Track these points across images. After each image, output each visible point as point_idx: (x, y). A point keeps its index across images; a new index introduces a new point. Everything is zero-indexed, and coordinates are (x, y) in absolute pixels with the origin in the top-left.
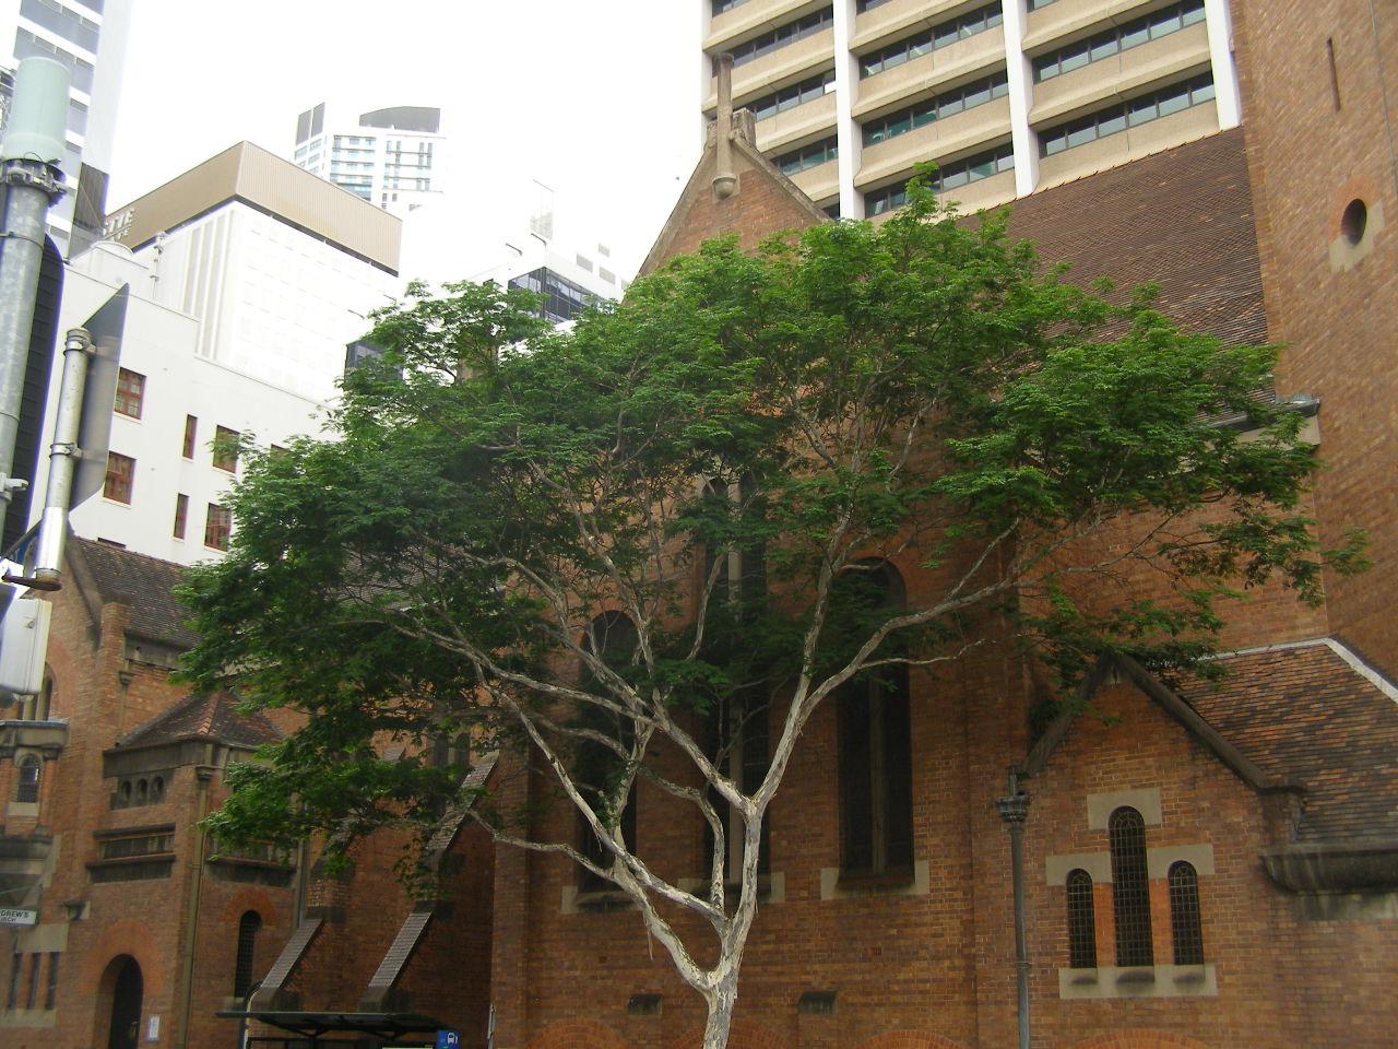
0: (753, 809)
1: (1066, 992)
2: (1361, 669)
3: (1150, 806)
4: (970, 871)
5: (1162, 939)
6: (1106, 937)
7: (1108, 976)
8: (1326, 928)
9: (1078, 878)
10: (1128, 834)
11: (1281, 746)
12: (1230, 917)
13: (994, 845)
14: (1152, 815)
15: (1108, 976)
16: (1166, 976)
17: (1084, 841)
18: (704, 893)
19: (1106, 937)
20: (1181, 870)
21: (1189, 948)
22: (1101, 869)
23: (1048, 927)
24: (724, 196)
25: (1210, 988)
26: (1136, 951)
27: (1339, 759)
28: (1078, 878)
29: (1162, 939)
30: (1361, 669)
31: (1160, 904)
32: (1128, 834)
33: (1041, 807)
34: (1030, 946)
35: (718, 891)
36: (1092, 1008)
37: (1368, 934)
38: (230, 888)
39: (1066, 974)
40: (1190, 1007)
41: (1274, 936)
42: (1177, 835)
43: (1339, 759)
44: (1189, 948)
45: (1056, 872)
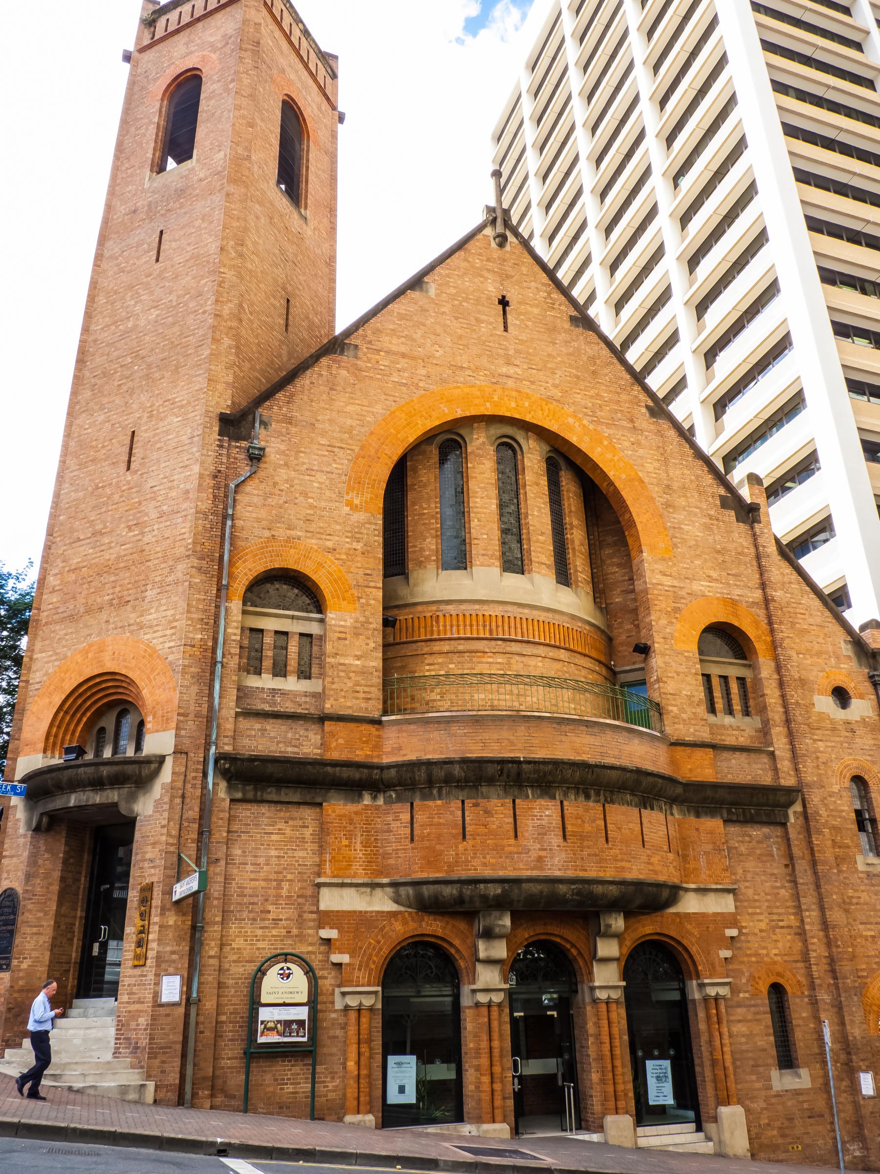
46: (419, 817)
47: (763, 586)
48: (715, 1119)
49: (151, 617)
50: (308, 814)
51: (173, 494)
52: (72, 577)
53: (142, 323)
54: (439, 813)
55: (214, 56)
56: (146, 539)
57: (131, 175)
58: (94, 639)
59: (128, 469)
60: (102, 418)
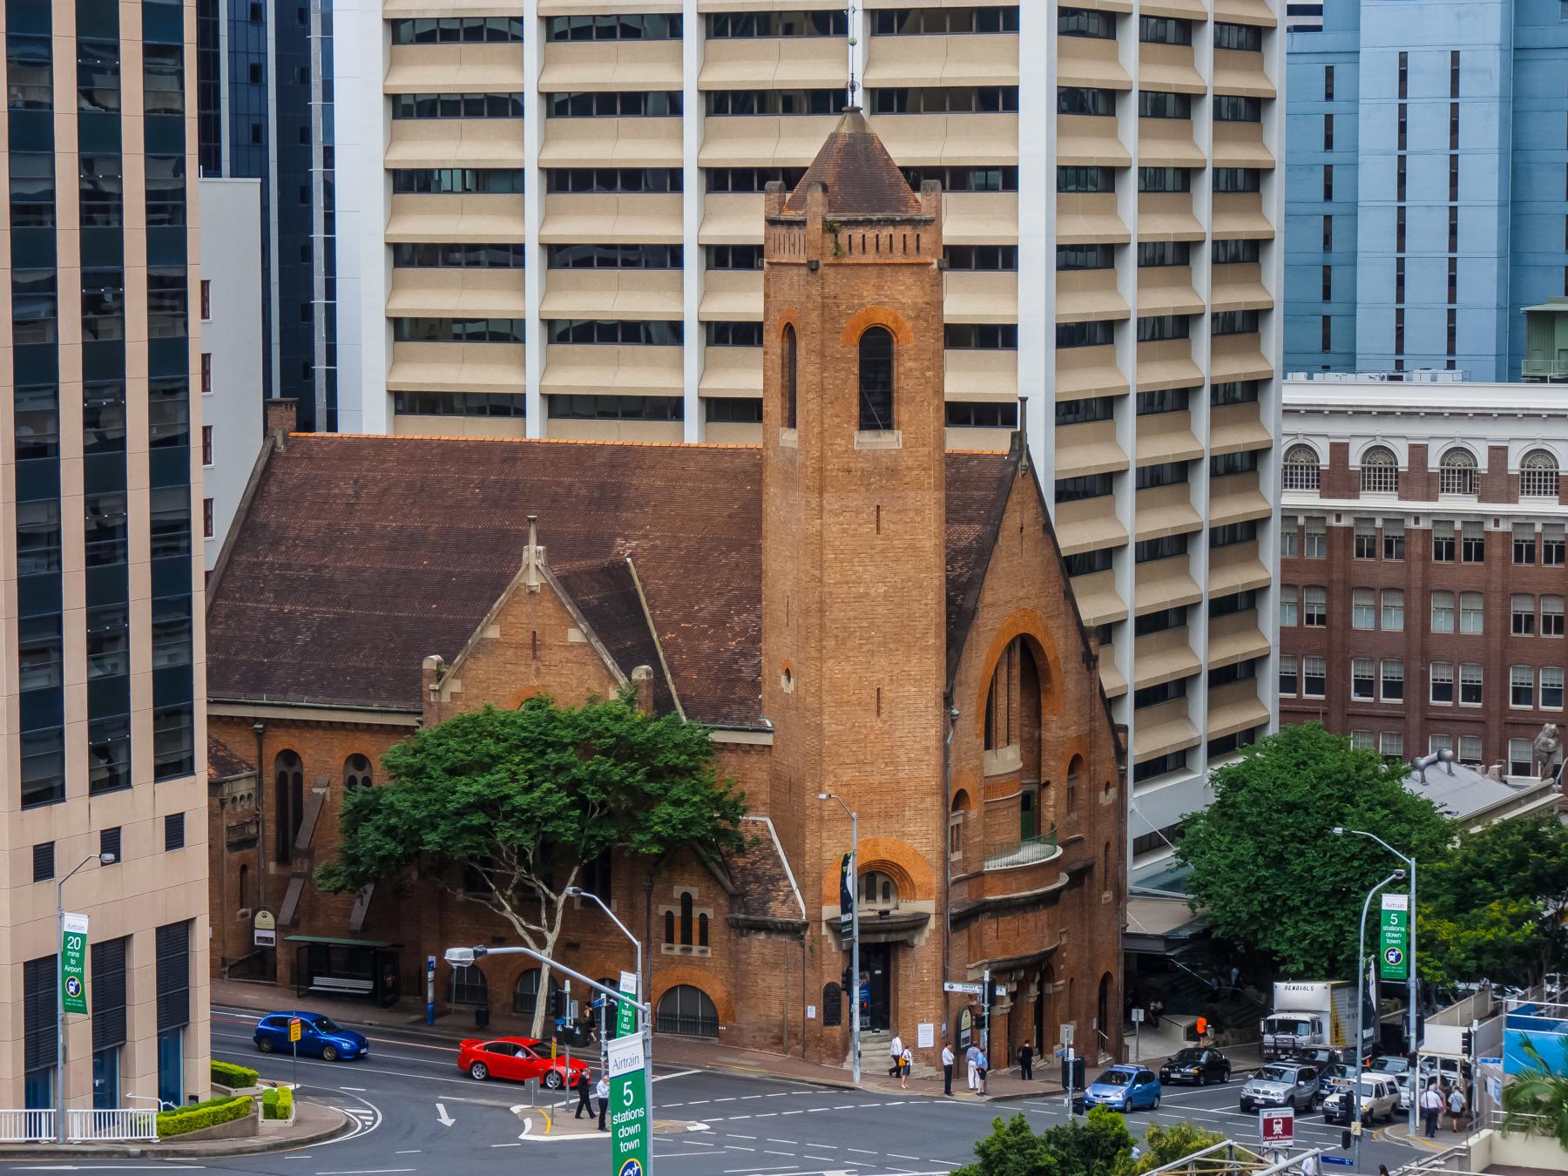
0: (561, 900)
1: (663, 951)
2: (775, 838)
3: (695, 893)
4: (632, 906)
5: (696, 938)
6: (678, 934)
7: (677, 949)
8: (744, 940)
9: (669, 914)
10: (687, 901)
11: (744, 869)
12: (717, 933)
13: (641, 900)
14: (695, 896)
15: (677, 949)
16: (696, 950)
17: (672, 901)
18: (539, 924)
19: (678, 934)
20: (703, 916)
21: (704, 941)
22: (677, 912)
23: (658, 929)
24: (532, 593)
25: (709, 955)
26: (687, 939)
27: (758, 879)
28: (669, 914)
29: (696, 938)
30: (775, 838)
31: (696, 926)
32: (687, 901)
33: (657, 887)
34: (653, 935)
35: (544, 922)
36: (672, 958)
37: (756, 943)
38: (236, 855)
39: (664, 946)
40: (702, 959)
41: (729, 940)
42: (702, 905)
43: (758, 879)
44: (704, 941)
45: (662, 910)
46: (1001, 926)
47: (1092, 719)
48: (1051, 1052)
49: (911, 828)
50: (965, 932)
51: (917, 746)
52: (845, 790)
53: (872, 592)
54: (1009, 923)
55: (909, 324)
56: (901, 775)
57: (838, 425)
58: (869, 836)
59: (879, 713)
60: (848, 669)
